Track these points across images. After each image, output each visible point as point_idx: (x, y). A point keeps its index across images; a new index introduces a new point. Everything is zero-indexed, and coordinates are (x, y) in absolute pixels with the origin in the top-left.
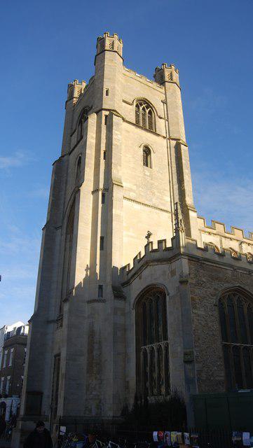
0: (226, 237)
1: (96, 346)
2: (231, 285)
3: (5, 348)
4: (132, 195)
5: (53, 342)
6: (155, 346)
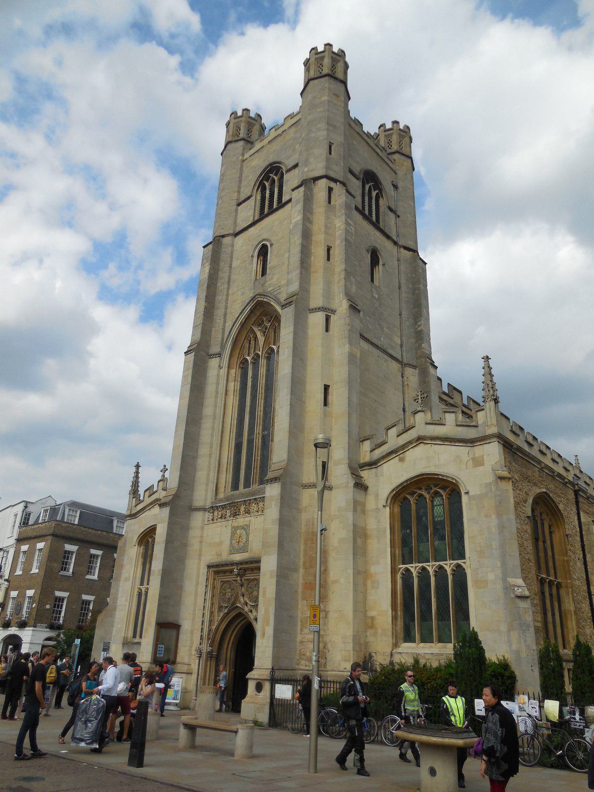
2: (539, 491)
3: (20, 540)
5: (201, 542)
6: (431, 567)
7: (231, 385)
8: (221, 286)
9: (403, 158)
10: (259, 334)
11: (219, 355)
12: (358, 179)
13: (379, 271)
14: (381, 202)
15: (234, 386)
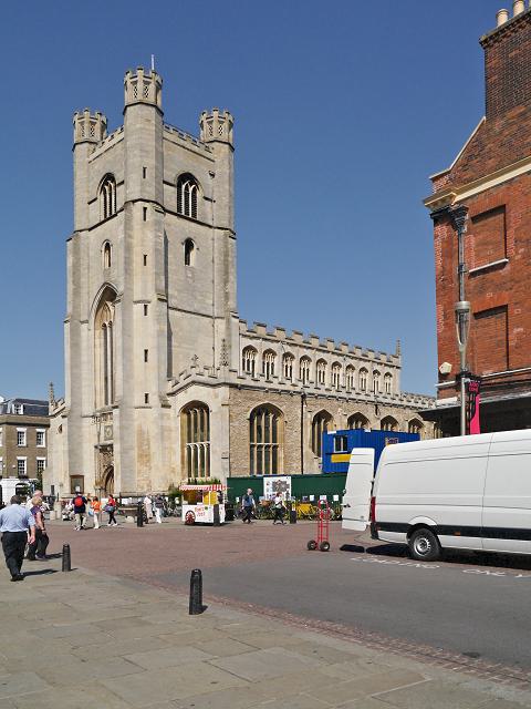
0: (266, 339)
1: (146, 443)
4: (172, 302)
7: (97, 341)
8: (84, 271)
9: (217, 144)
10: (111, 308)
11: (87, 322)
12: (171, 185)
13: (193, 254)
14: (199, 194)
15: (100, 341)
